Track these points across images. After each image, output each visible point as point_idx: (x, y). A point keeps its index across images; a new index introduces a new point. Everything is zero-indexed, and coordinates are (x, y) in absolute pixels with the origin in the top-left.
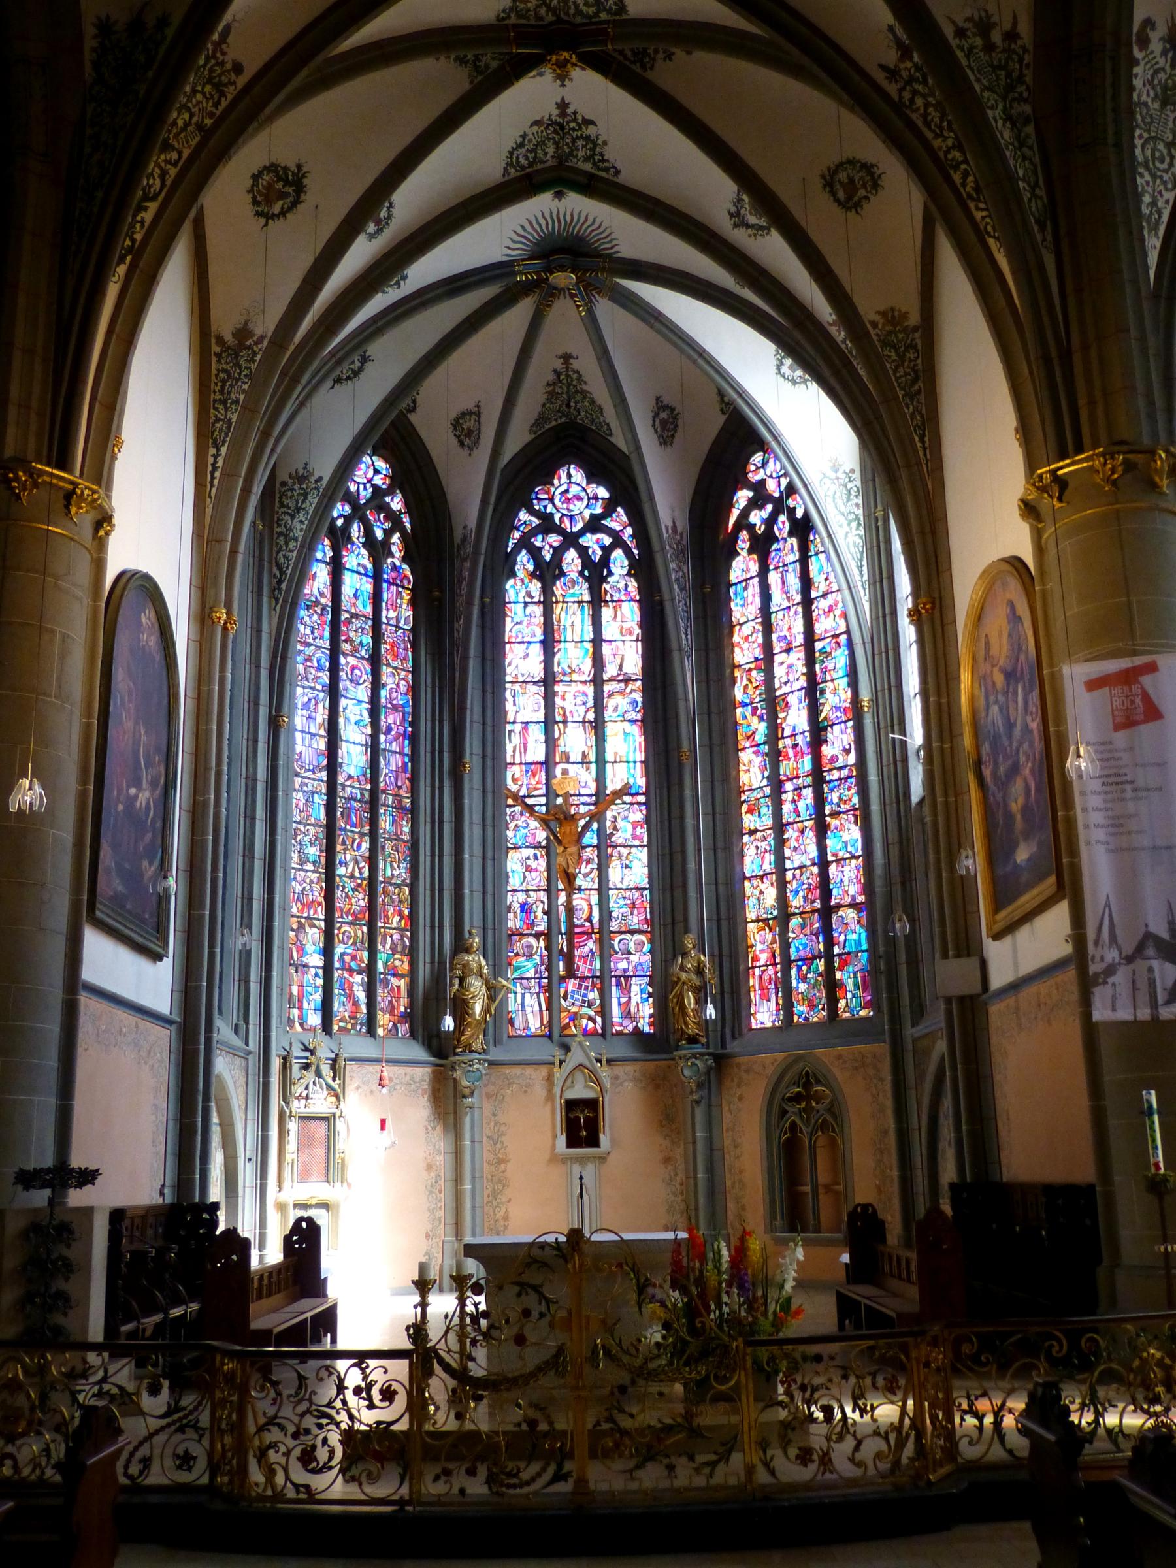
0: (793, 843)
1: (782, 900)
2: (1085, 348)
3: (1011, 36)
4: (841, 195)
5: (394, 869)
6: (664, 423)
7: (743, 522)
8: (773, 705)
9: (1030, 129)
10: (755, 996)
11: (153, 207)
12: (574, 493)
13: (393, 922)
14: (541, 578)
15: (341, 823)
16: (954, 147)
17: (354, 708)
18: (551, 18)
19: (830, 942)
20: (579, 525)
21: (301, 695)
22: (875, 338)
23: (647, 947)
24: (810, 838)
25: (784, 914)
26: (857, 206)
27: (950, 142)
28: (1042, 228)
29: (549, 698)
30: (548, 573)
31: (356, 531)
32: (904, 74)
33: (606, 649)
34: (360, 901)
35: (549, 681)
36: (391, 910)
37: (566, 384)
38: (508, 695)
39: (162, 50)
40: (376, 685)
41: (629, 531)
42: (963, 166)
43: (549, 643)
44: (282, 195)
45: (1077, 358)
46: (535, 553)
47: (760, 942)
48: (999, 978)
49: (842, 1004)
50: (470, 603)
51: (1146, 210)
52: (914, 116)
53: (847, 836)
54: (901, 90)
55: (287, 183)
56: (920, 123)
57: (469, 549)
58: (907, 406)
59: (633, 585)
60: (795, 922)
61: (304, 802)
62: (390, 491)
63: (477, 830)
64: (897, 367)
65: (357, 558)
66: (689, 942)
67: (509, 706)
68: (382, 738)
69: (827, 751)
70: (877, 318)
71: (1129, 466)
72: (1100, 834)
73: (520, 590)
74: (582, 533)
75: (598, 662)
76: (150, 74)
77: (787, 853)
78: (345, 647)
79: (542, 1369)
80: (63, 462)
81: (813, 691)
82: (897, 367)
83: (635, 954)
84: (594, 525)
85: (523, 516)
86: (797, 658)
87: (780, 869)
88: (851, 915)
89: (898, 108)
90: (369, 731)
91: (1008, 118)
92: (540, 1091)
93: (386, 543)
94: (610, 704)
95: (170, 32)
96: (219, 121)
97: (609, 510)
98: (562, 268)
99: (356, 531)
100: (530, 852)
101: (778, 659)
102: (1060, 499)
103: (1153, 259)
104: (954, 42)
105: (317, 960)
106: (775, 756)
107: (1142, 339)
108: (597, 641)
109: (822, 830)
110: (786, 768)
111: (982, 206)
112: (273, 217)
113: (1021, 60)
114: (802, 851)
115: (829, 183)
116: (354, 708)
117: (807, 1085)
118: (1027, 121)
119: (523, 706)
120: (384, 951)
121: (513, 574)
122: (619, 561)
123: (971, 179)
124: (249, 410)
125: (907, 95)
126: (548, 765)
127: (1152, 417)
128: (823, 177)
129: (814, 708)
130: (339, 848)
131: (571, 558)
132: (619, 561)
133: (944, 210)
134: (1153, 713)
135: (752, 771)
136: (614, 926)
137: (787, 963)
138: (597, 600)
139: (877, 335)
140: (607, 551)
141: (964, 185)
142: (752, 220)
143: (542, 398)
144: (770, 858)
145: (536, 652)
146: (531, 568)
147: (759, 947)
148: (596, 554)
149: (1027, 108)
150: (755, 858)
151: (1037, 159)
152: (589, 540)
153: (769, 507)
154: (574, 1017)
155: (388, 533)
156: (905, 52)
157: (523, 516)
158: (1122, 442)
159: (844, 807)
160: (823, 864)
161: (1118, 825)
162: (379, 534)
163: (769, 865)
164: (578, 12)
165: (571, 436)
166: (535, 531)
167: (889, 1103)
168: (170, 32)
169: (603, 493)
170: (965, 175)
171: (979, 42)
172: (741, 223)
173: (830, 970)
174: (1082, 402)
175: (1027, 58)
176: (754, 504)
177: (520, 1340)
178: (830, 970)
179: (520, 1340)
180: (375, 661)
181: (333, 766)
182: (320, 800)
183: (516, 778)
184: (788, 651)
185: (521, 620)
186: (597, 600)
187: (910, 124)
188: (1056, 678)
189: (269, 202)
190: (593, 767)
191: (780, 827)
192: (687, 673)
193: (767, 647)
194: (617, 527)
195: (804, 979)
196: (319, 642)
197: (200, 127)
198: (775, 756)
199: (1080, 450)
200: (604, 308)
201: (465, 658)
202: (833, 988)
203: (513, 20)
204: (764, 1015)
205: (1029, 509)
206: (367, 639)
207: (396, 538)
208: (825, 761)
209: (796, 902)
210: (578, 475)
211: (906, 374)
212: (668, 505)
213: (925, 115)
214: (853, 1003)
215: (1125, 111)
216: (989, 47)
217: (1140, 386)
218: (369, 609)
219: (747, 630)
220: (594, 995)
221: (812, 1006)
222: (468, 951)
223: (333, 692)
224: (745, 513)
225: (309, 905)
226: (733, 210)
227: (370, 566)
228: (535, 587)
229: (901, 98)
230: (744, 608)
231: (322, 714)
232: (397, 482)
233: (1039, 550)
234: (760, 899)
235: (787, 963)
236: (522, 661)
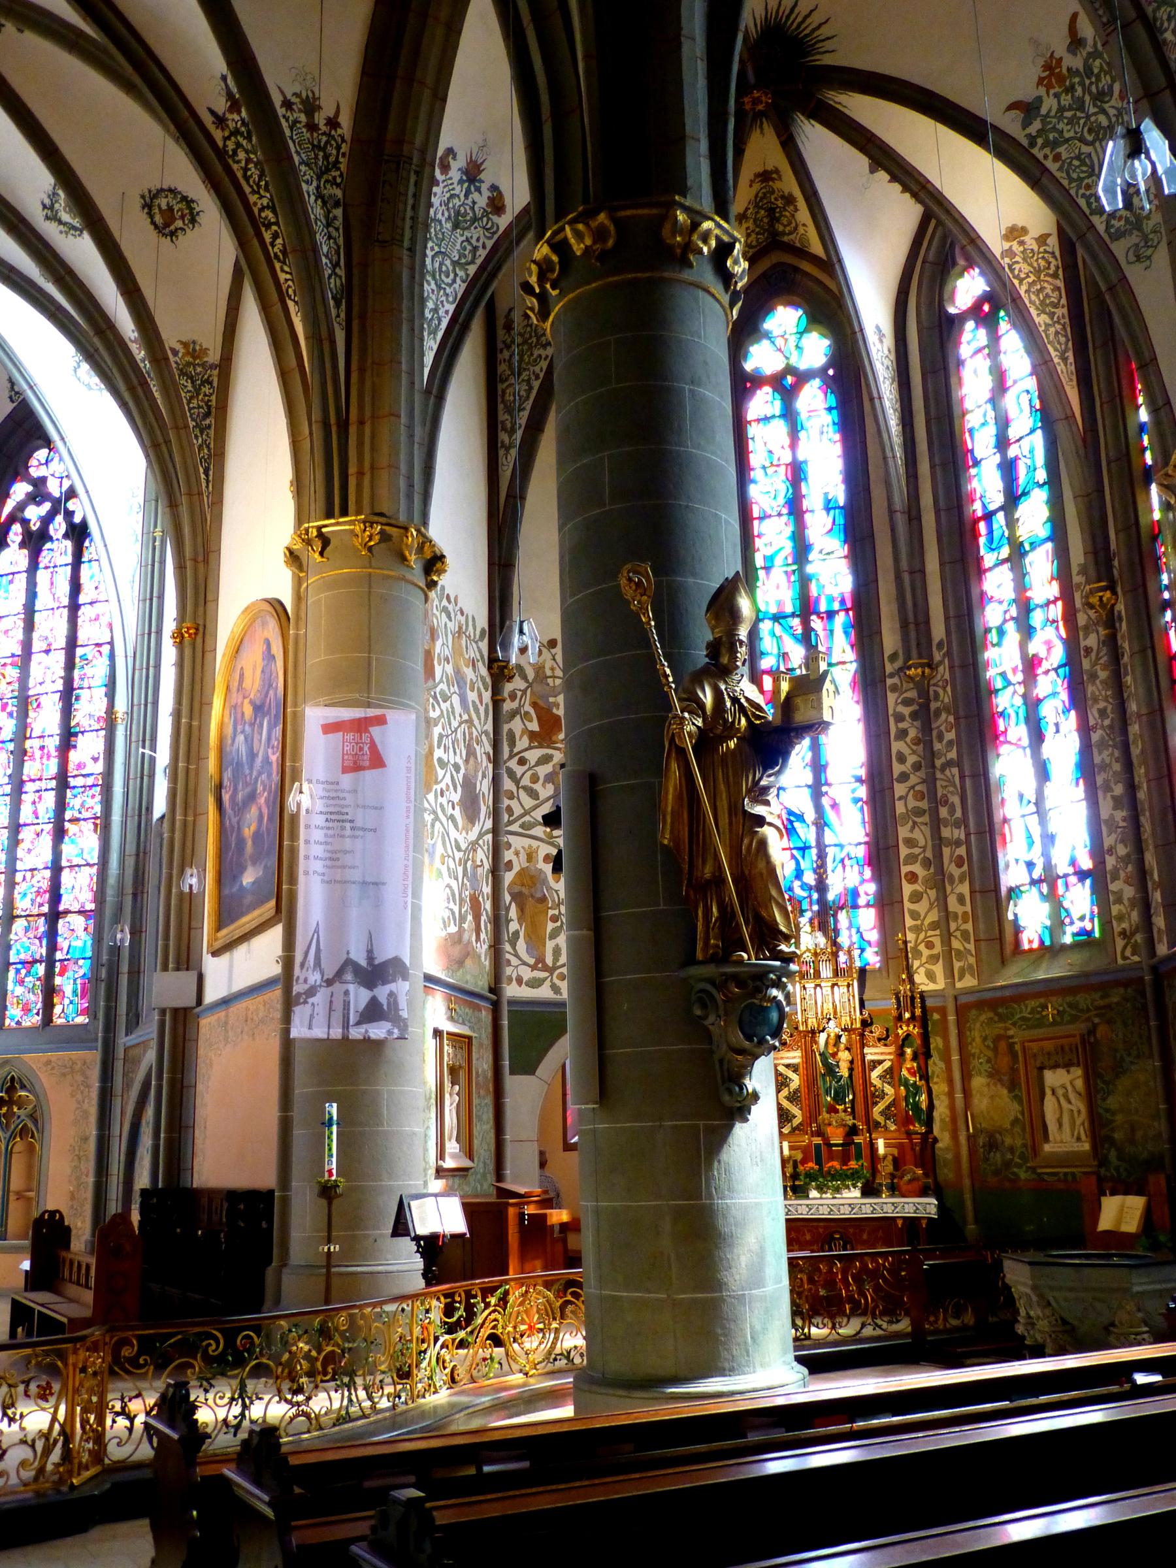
2: (361, 423)
3: (333, 123)
4: (158, 219)
9: (338, 212)
16: (268, 207)
22: (174, 365)
26: (173, 234)
27: (265, 202)
28: (338, 306)
32: (232, 125)
42: (274, 228)
45: (353, 430)
48: (210, 996)
51: (428, 315)
52: (235, 167)
54: (226, 139)
56: (239, 174)
58: (196, 437)
64: (192, 398)
70: (178, 347)
71: (385, 537)
72: (318, 866)
81: (68, 695)
82: (192, 398)
89: (221, 154)
91: (319, 196)
102: (321, 554)
103: (429, 359)
104: (281, 111)
107: (410, 427)
111: (286, 269)
113: (338, 148)
115: (148, 203)
118: (337, 204)
123: (279, 241)
125: (231, 145)
127: (410, 497)
128: (143, 197)
134: (378, 761)
139: (176, 363)
141: (273, 245)
142: (66, 217)
149: (339, 193)
151: (341, 241)
153: (47, 506)
156: (234, 106)
158: (381, 515)
161: (334, 859)
170: (275, 236)
171: (303, 118)
174: (352, 470)
175: (344, 148)
188: (298, 718)
193: (27, 645)
199: (344, 512)
205: (293, 557)
211: (199, 407)
213: (246, 170)
215: (421, 225)
216: (312, 127)
217: (403, 468)
224: (21, 507)
226: (47, 202)
229: (225, 146)
233: (298, 598)
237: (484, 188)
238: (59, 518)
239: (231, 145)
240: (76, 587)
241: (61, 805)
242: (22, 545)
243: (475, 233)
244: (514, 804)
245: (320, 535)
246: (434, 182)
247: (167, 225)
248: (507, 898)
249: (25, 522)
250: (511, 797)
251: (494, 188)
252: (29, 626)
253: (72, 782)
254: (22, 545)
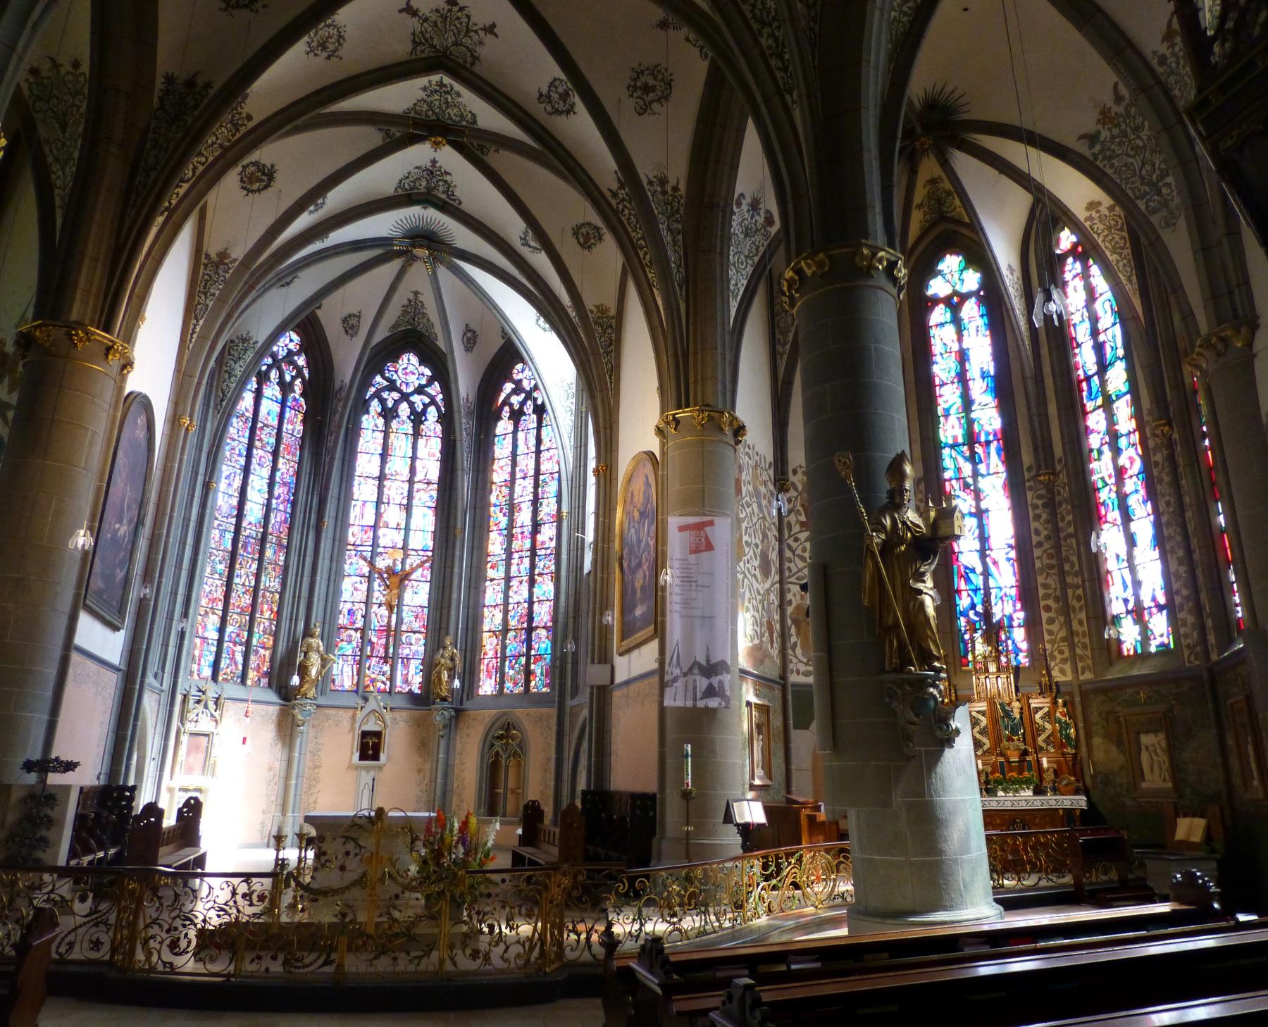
0: (514, 589)
1: (505, 621)
2: (696, 353)
4: (582, 240)
5: (271, 582)
6: (469, 340)
7: (506, 402)
8: (512, 508)
9: (680, 237)
10: (483, 675)
11: (186, 186)
12: (409, 370)
14: (384, 417)
15: (241, 551)
17: (258, 482)
18: (434, 117)
19: (529, 648)
20: (411, 389)
21: (225, 470)
23: (423, 642)
24: (525, 586)
25: (505, 629)
26: (590, 247)
29: (380, 488)
30: (389, 414)
31: (274, 374)
33: (418, 464)
34: (247, 600)
35: (381, 478)
36: (265, 607)
37: (414, 308)
38: (356, 483)
39: (206, 101)
40: (274, 469)
41: (441, 396)
43: (384, 456)
44: (261, 181)
45: (691, 358)
46: (383, 402)
47: (489, 644)
48: (619, 679)
49: (533, 684)
50: (340, 427)
51: (732, 288)
53: (546, 588)
55: (264, 174)
57: (343, 395)
59: (439, 428)
60: (511, 634)
62: (298, 353)
63: (327, 563)
65: (272, 390)
66: (448, 641)
67: (355, 490)
68: (274, 501)
69: (539, 538)
71: (710, 418)
72: (677, 607)
73: (371, 421)
74: (412, 394)
75: (413, 470)
76: (196, 113)
77: (511, 593)
78: (258, 444)
79: (353, 884)
80: (107, 328)
81: (536, 502)
83: (415, 646)
84: (420, 390)
85: (378, 379)
86: (529, 483)
87: (506, 603)
88: (543, 633)
89: (615, 212)
90: (266, 496)
91: (669, 229)
92: (346, 724)
93: (291, 384)
94: (417, 496)
95: (212, 92)
96: (234, 145)
97: (430, 382)
98: (421, 246)
99: (274, 374)
100: (358, 579)
101: (518, 482)
103: (733, 312)
104: (647, 187)
106: (510, 537)
107: (723, 354)
108: (414, 458)
109: (532, 583)
110: (516, 545)
112: (252, 191)
114: (519, 593)
115: (576, 233)
116: (258, 482)
117: (508, 730)
118: (679, 233)
119: (363, 490)
120: (258, 630)
121: (367, 412)
122: (432, 413)
124: (221, 301)
125: (620, 207)
126: (375, 527)
127: (724, 394)
129: (535, 512)
130: (237, 566)
131: (404, 409)
132: (432, 413)
133: (633, 267)
134: (709, 547)
135: (495, 544)
136: (404, 628)
137: (504, 658)
138: (417, 434)
140: (426, 406)
142: (532, 243)
143: (399, 313)
144: (501, 596)
145: (377, 460)
146: (379, 410)
147: (488, 647)
148: (420, 408)
149: (680, 226)
150: (492, 594)
152: (416, 399)
153: (523, 395)
154: (373, 681)
155: (294, 378)
156: (622, 186)
157: (378, 379)
158: (708, 405)
159: (546, 571)
160: (531, 602)
161: (686, 603)
162: (288, 378)
163: (500, 599)
164: (450, 118)
165: (413, 337)
166: (384, 389)
167: (553, 743)
168: (212, 92)
169: (428, 372)
170: (646, 254)
171: (659, 189)
172: (526, 244)
173: (528, 664)
174: (691, 380)
175: (682, 201)
176: (515, 392)
177: (342, 868)
178: (528, 664)
179: (342, 868)
180: (275, 454)
181: (240, 516)
182: (229, 536)
183: (355, 534)
184: (524, 478)
186: (417, 434)
187: (621, 222)
188: (664, 522)
189: (251, 182)
190: (403, 532)
191: (508, 579)
192: (465, 483)
193: (513, 474)
194: (433, 393)
195: (513, 668)
196: (242, 439)
197: (221, 146)
198: (510, 537)
199: (688, 406)
200: (443, 272)
201: (332, 459)
202: (528, 674)
203: (413, 114)
204: (487, 687)
205: (660, 431)
206: (273, 441)
207: (298, 382)
208: (538, 543)
209: (513, 623)
210: (414, 360)
212: (465, 386)
213: (629, 219)
214: (539, 684)
215: (726, 239)
216: (664, 193)
217: (720, 377)
218: (275, 423)
219: (502, 463)
220: (387, 668)
221: (516, 684)
222: (312, 636)
223: (246, 470)
224: (509, 396)
225: (214, 600)
227: (280, 397)
228: (381, 421)
230: (502, 449)
231: (237, 483)
232: (304, 348)
233: (663, 453)
234: (492, 619)
235: (504, 658)
236: (366, 464)
237: (762, 212)
238: (529, 402)
239: (620, 207)
240: (539, 441)
241: (533, 566)
242: (510, 418)
243: (758, 238)
244: (792, 565)
245: (675, 419)
246: (733, 213)
247: (586, 242)
248: (789, 622)
249: (511, 405)
250: (790, 561)
251: (768, 212)
252: (514, 464)
253: (539, 553)
254: (510, 418)
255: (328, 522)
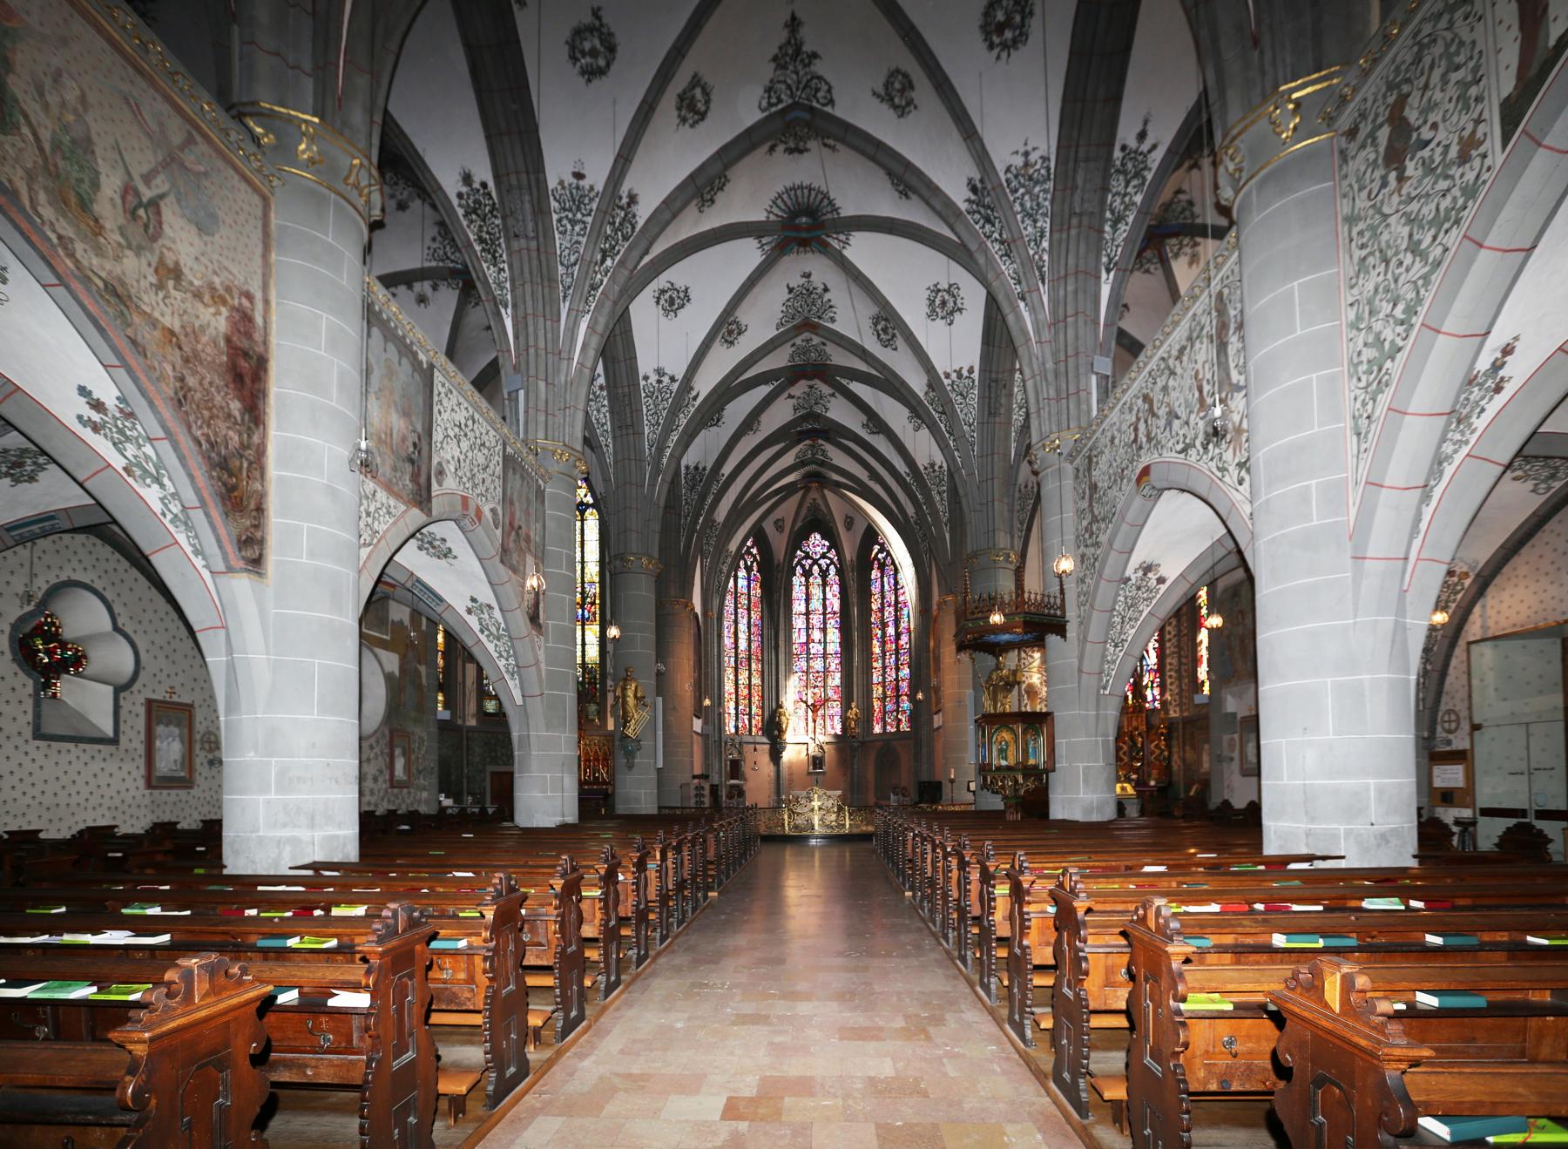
5: (756, 680)
7: (876, 557)
8: (884, 625)
12: (816, 544)
13: (756, 699)
17: (743, 627)
21: (726, 624)
29: (808, 619)
30: (807, 574)
34: (746, 692)
35: (808, 613)
37: (814, 508)
43: (808, 600)
61: (729, 661)
65: (742, 573)
73: (798, 580)
84: (824, 556)
86: (891, 609)
97: (829, 549)
105: (733, 712)
108: (825, 599)
110: (888, 646)
116: (743, 627)
119: (799, 623)
122: (832, 569)
126: (807, 643)
129: (897, 626)
132: (832, 569)
138: (825, 584)
152: (822, 562)
176: (880, 551)
180: (749, 610)
181: (736, 648)
185: (798, 591)
186: (825, 584)
191: (884, 668)
210: (818, 536)
212: (849, 553)
230: (875, 589)
234: (877, 691)
236: (799, 607)
252: (883, 597)
255: (781, 643)
